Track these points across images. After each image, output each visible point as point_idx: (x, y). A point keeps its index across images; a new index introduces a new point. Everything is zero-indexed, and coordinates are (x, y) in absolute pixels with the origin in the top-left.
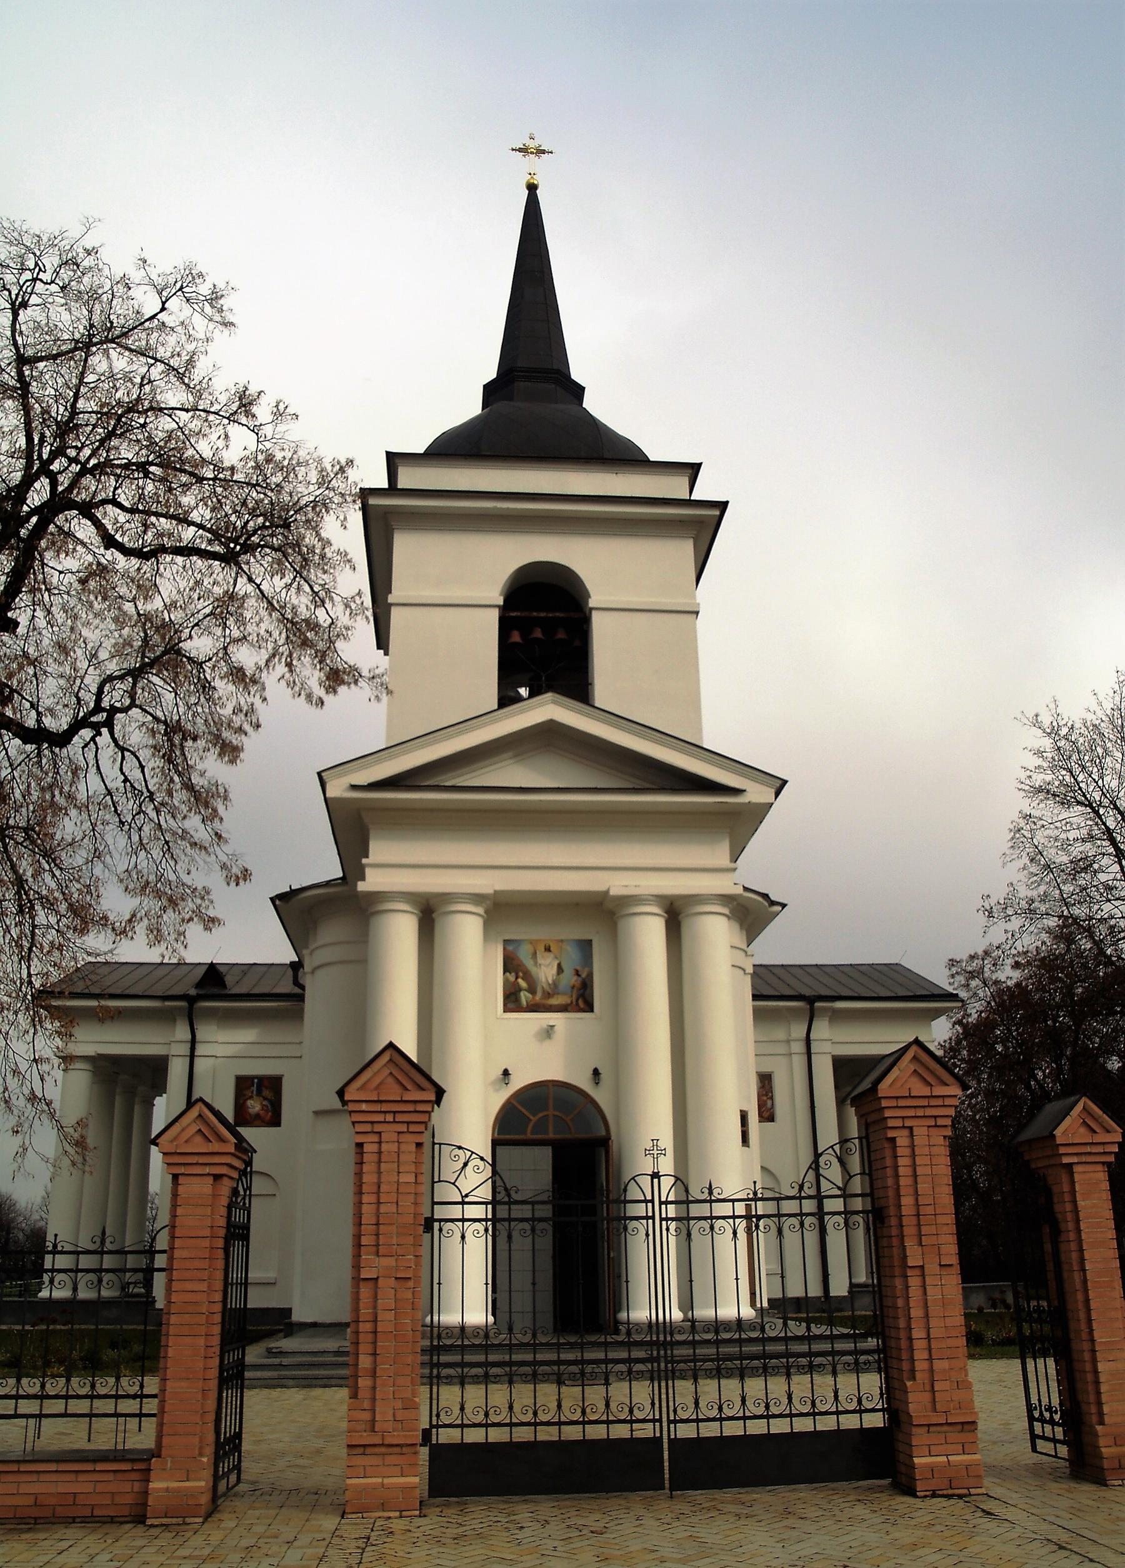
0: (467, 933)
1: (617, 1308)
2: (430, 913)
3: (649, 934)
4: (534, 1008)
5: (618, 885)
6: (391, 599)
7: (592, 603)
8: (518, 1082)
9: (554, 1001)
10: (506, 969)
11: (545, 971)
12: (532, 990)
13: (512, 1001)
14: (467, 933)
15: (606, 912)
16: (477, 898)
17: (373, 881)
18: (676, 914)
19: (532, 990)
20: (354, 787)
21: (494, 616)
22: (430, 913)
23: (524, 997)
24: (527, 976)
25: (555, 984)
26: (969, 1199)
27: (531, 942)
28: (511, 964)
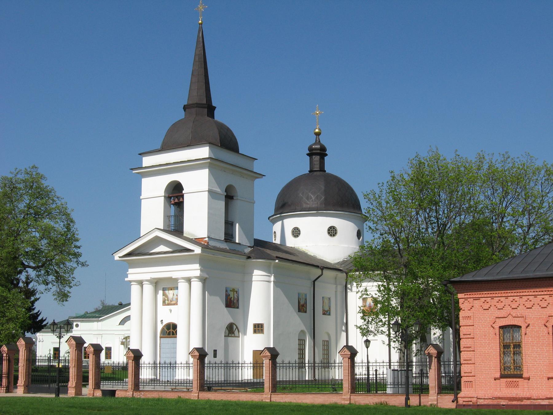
3: (183, 286)
4: (168, 304)
5: (174, 275)
6: (141, 197)
7: (184, 192)
8: (165, 323)
9: (172, 303)
12: (168, 300)
13: (164, 303)
17: (130, 278)
18: (189, 280)
19: (168, 300)
20: (120, 257)
21: (162, 199)
23: (167, 302)
24: (167, 297)
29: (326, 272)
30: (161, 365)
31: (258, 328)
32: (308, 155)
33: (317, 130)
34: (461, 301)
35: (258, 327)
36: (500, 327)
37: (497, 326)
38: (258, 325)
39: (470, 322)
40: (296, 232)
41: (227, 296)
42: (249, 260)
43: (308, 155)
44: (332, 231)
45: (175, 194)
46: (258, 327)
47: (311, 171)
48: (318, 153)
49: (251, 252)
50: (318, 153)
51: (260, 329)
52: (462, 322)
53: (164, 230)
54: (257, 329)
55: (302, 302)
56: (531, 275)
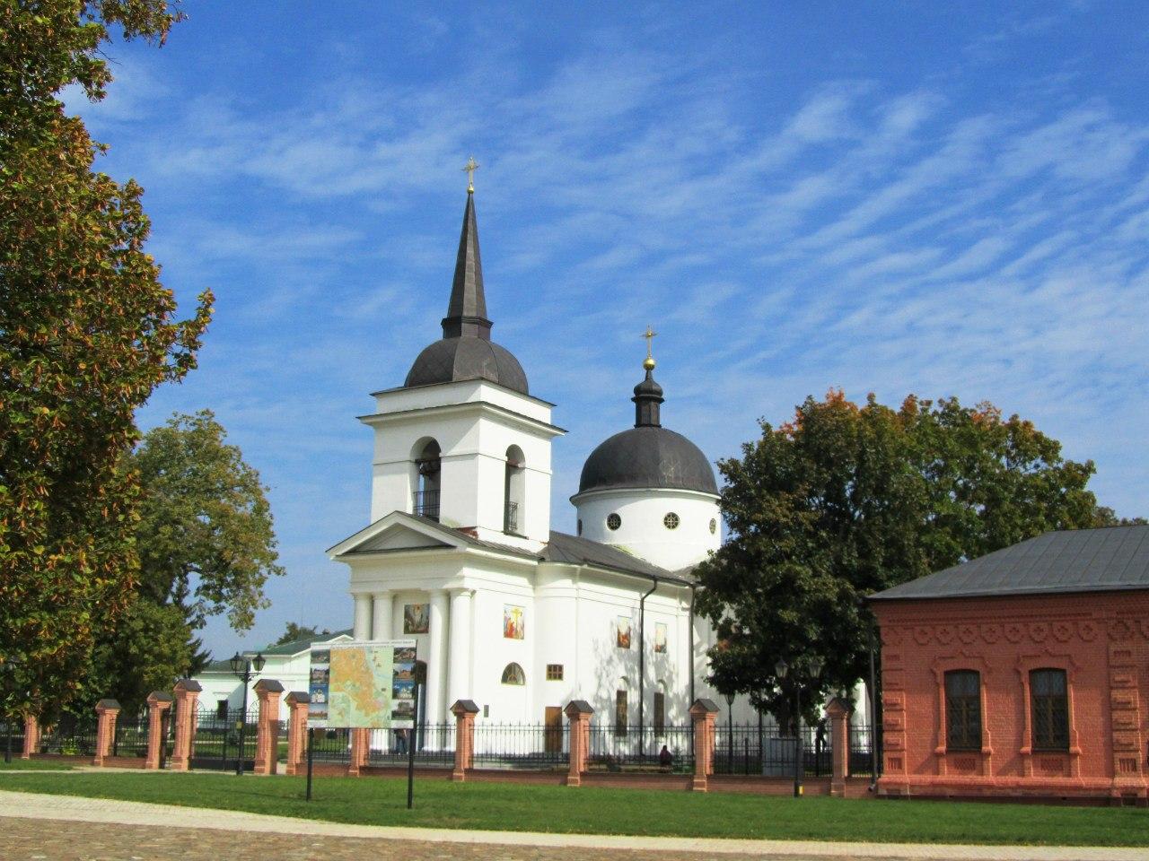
0: (383, 607)
1: (422, 744)
2: (372, 600)
4: (414, 632)
7: (441, 455)
10: (405, 617)
11: (417, 618)
12: (413, 624)
14: (383, 607)
15: (427, 594)
16: (383, 593)
19: (413, 624)
21: (408, 466)
22: (372, 600)
23: (410, 627)
24: (411, 619)
25: (420, 623)
26: (144, 718)
27: (414, 606)
28: (407, 615)
29: (659, 583)
30: (512, 728)
31: (555, 672)
32: (633, 400)
33: (651, 362)
34: (883, 631)
35: (555, 670)
36: (947, 673)
37: (940, 673)
38: (555, 666)
39: (896, 664)
40: (615, 522)
41: (507, 619)
42: (544, 565)
43: (633, 400)
44: (672, 521)
45: (514, 462)
46: (555, 670)
47: (637, 425)
48: (647, 398)
49: (545, 550)
50: (647, 398)
51: (558, 672)
52: (885, 664)
53: (414, 517)
54: (552, 672)
55: (623, 632)
56: (995, 590)
